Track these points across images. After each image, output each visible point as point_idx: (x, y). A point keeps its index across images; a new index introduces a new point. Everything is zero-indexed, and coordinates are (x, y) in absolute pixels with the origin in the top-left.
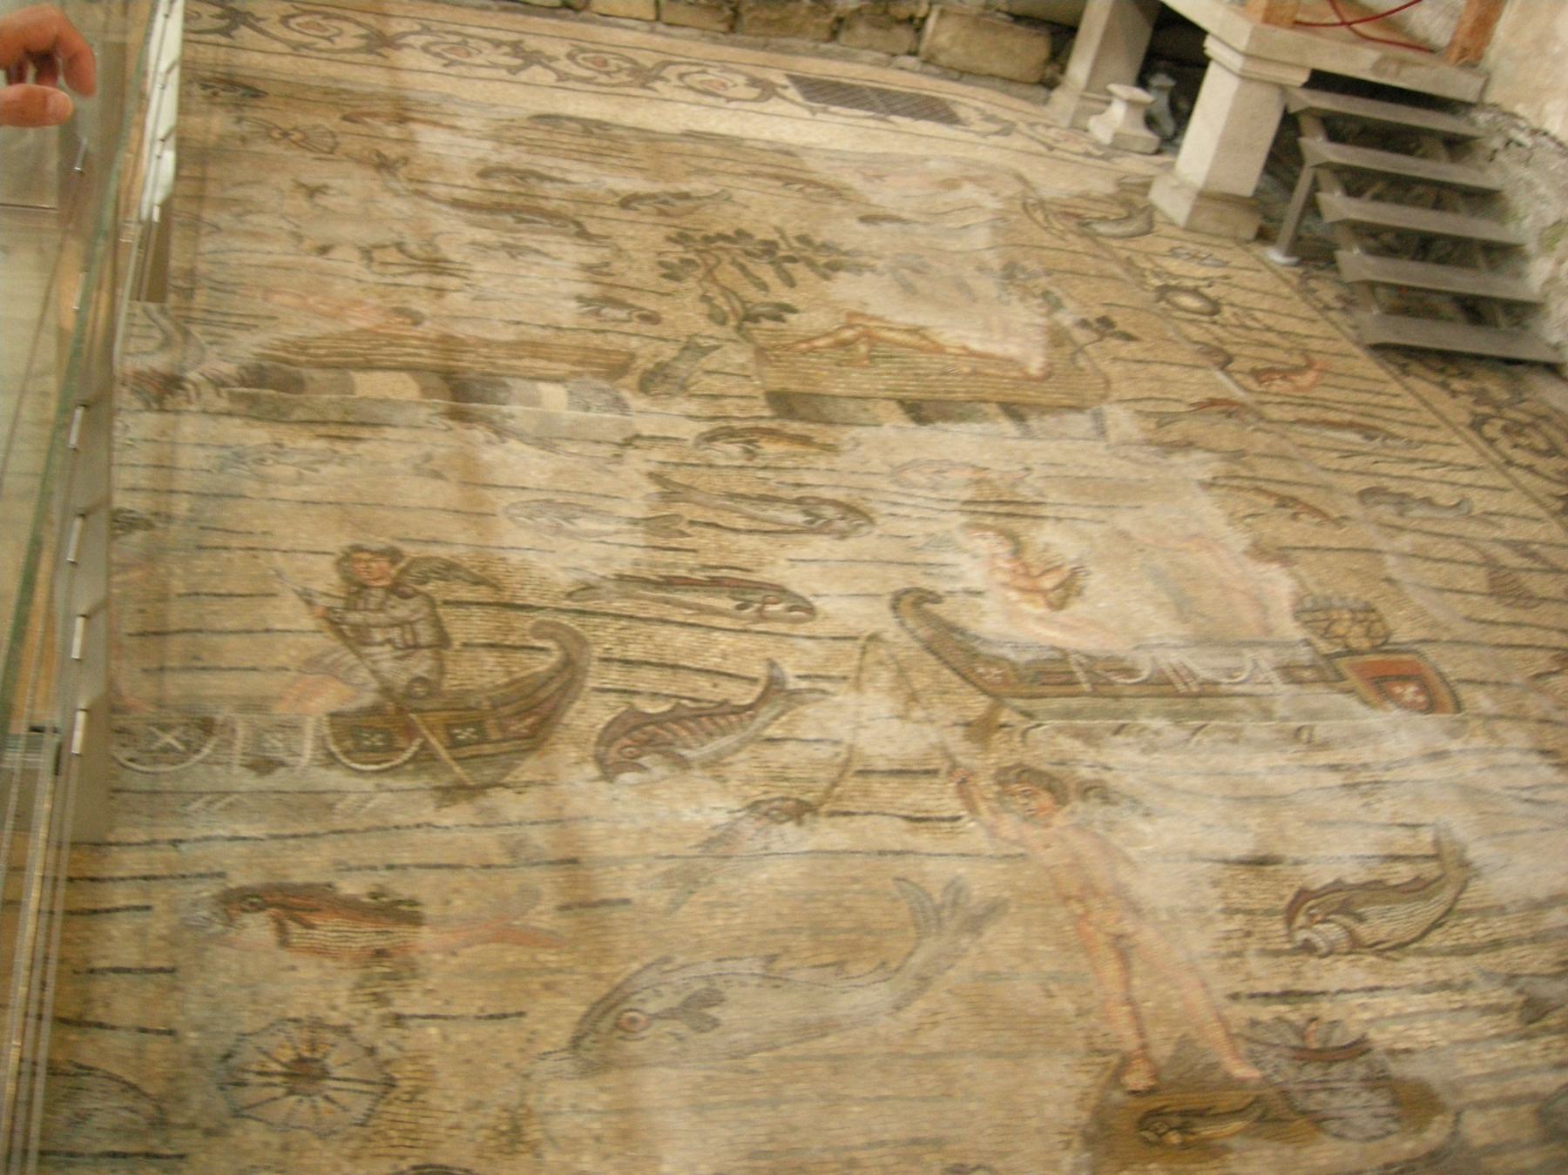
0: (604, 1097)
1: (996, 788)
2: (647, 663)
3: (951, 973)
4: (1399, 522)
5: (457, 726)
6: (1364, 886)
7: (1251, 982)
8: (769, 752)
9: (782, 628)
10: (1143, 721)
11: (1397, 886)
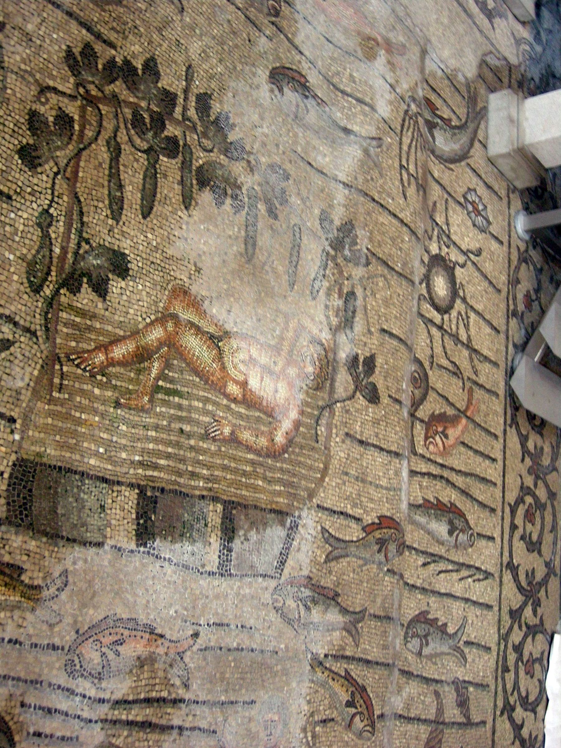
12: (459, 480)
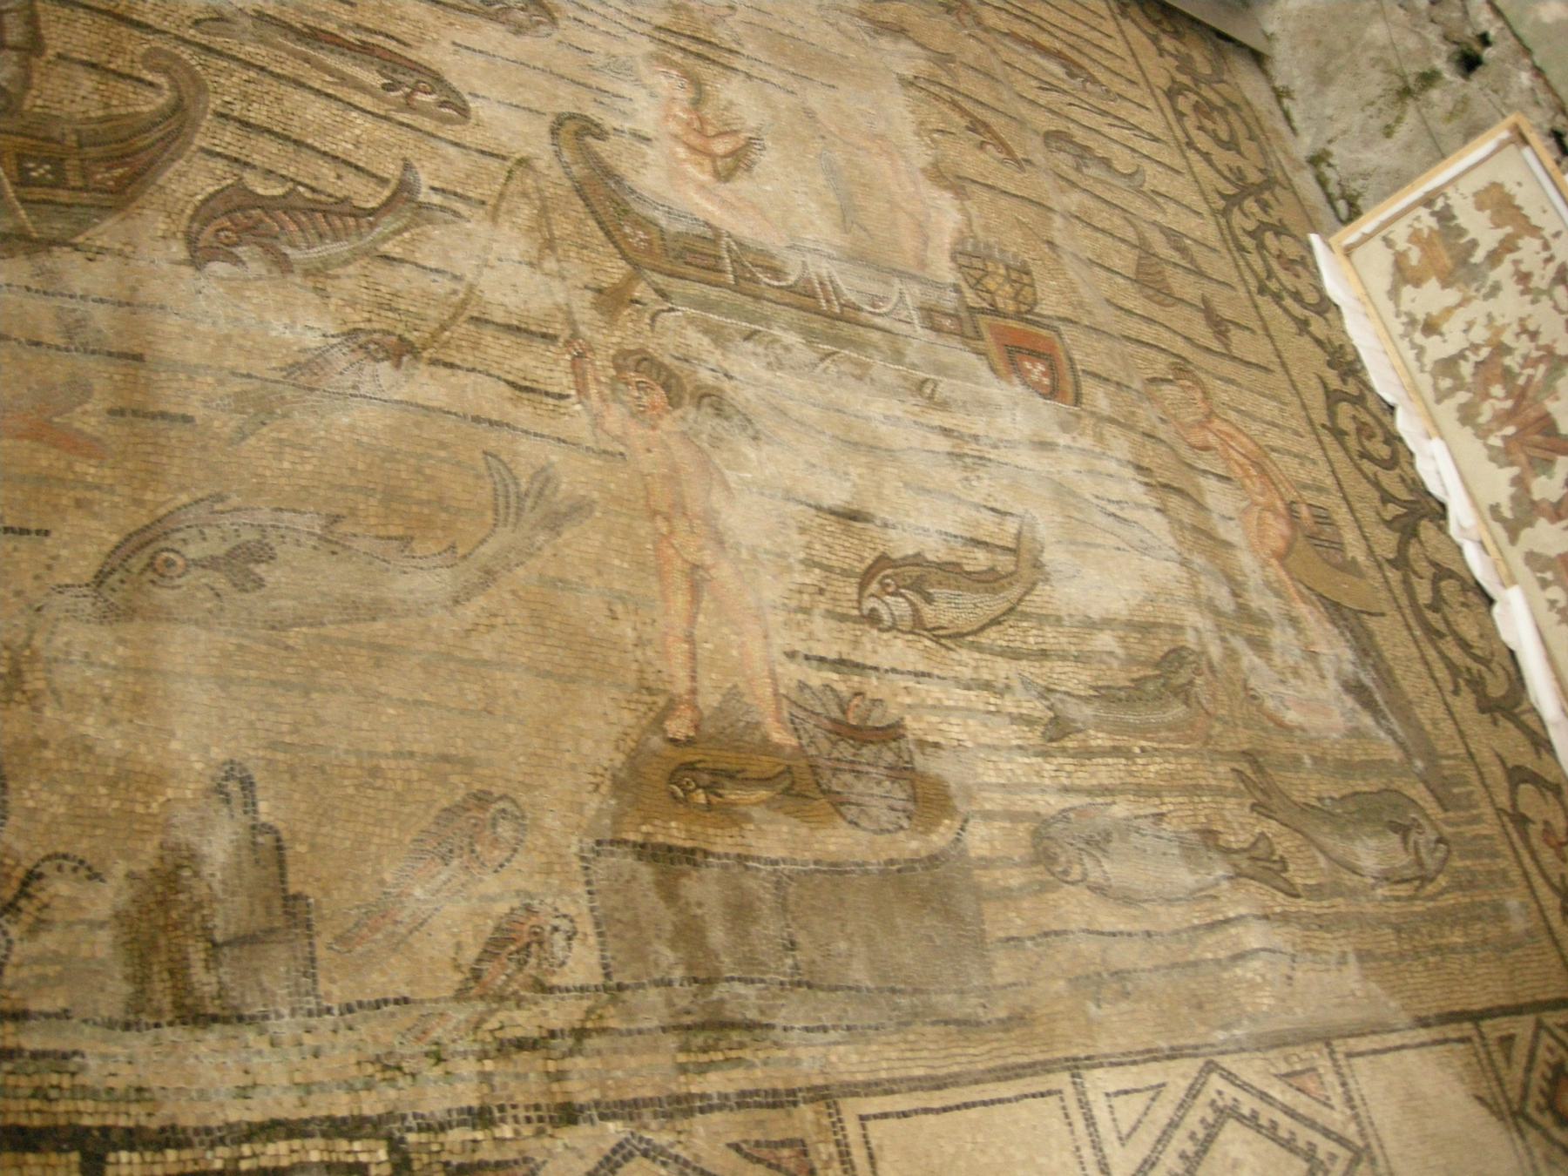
0: (120, 650)
1: (612, 372)
2: (269, 131)
3: (520, 571)
4: (1074, 176)
5: (34, 159)
6: (940, 566)
7: (812, 644)
8: (382, 273)
9: (428, 125)
10: (776, 332)
11: (969, 573)
12: (1059, 34)
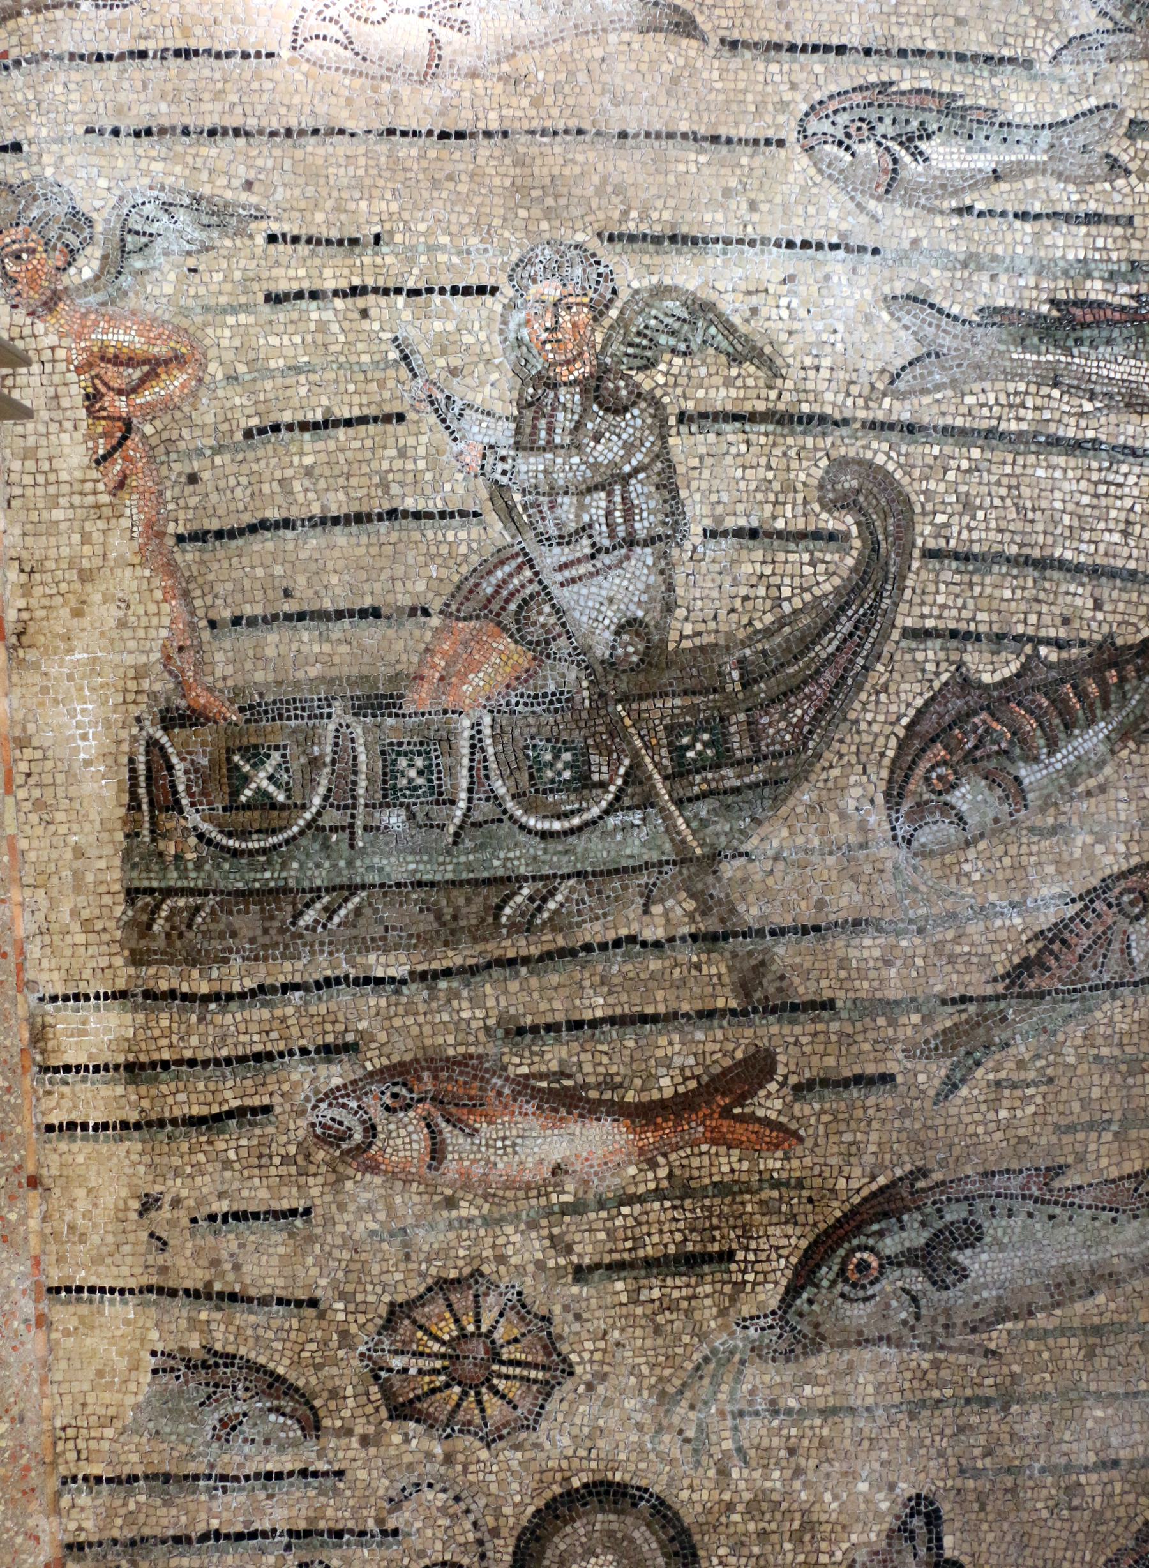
2: (999, 558)
